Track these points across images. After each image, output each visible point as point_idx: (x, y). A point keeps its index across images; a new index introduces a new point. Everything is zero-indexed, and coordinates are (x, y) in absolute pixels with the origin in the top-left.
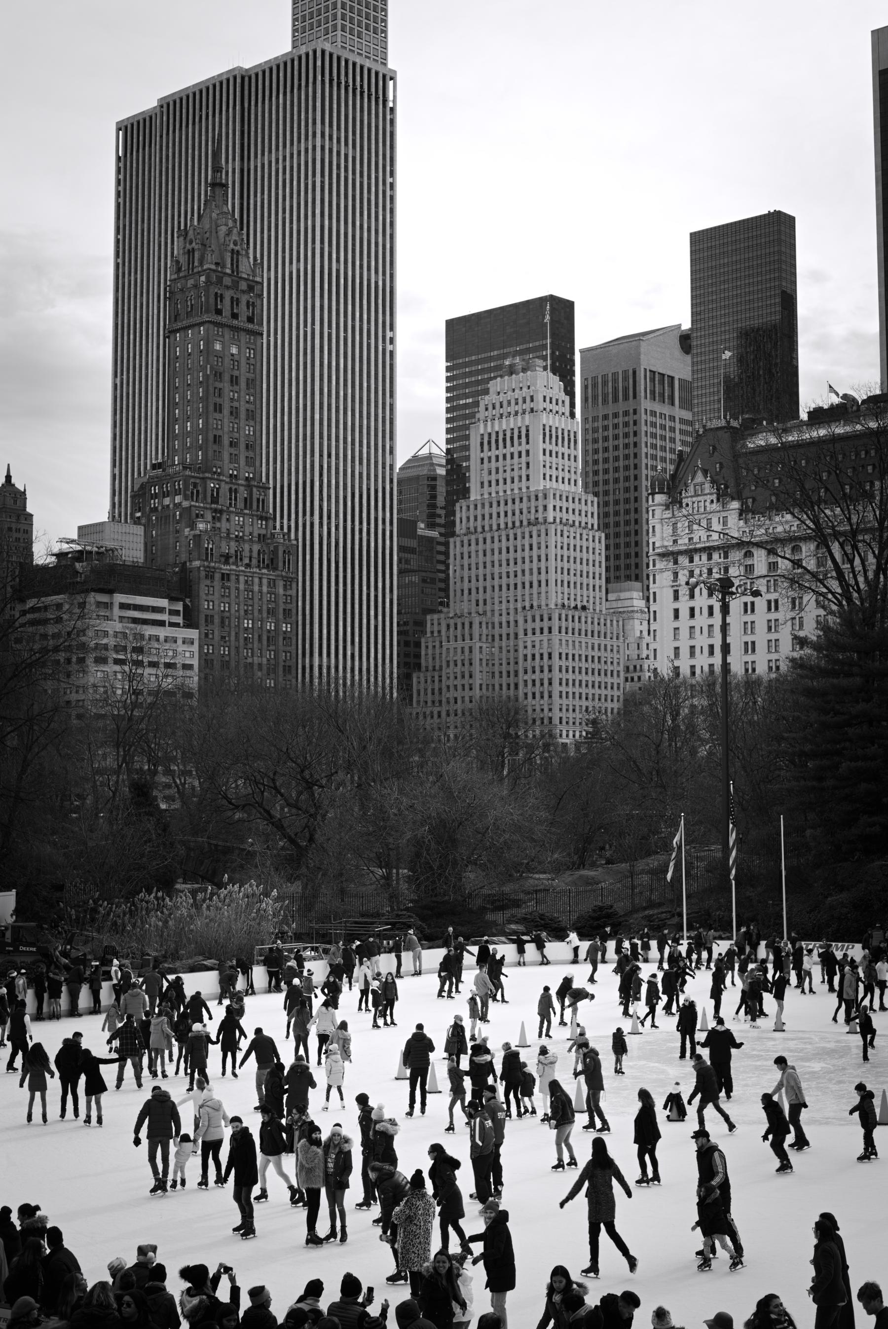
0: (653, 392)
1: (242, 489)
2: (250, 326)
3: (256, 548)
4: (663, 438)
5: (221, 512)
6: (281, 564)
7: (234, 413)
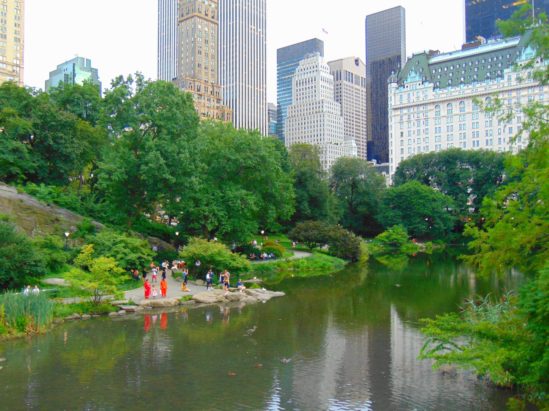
0: (346, 78)
1: (210, 87)
2: (213, 20)
3: (216, 111)
4: (350, 94)
5: (201, 95)
6: (226, 119)
7: (207, 55)
